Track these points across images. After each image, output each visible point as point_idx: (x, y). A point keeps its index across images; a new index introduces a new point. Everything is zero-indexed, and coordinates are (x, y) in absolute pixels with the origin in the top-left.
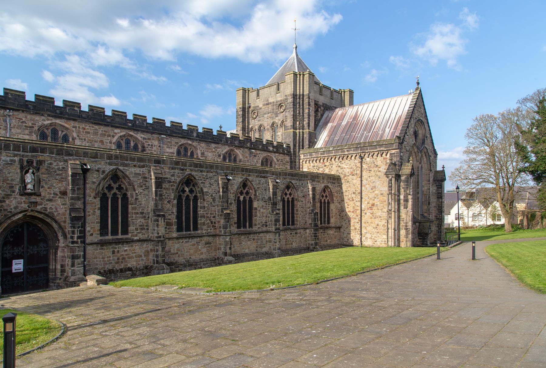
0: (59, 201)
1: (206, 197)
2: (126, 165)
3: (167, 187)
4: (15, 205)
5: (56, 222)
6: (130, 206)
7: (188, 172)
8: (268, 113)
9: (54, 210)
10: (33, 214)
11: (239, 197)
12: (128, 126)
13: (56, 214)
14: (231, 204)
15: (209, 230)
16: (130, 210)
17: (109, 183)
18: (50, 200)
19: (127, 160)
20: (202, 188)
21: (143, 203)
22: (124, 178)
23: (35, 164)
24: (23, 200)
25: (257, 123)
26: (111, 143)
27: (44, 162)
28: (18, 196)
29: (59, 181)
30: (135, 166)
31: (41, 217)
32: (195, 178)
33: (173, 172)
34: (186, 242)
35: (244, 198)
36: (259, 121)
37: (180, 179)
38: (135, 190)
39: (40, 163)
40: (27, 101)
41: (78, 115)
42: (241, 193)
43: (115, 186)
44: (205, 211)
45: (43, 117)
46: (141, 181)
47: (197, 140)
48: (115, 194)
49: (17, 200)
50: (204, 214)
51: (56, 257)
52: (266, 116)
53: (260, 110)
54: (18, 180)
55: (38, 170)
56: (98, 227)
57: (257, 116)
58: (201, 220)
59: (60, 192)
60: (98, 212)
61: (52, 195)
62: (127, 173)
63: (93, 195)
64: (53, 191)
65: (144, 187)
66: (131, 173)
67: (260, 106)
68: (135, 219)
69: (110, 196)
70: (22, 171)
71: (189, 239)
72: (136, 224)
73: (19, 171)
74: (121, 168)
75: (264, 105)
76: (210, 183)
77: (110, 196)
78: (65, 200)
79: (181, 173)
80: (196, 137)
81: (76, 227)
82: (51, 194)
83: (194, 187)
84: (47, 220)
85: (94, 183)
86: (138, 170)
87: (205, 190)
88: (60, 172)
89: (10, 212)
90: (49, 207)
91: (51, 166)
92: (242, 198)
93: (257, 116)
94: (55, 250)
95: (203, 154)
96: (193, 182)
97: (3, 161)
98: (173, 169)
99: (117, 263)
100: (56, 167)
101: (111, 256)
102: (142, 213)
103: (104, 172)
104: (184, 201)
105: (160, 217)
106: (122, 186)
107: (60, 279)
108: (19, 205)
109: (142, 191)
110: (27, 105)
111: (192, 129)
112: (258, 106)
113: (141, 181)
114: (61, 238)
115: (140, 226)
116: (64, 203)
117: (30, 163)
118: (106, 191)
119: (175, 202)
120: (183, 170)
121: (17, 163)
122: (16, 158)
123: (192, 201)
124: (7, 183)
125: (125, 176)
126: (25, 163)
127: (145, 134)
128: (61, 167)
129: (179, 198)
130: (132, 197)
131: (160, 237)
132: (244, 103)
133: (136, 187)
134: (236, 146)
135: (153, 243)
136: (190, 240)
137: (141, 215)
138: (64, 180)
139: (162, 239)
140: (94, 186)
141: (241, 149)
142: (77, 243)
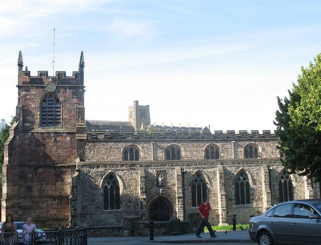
3: (228, 177)
7: (240, 168)
11: (280, 181)
14: (274, 185)
26: (202, 151)
30: (208, 168)
35: (285, 181)
42: (282, 178)
56: (190, 202)
60: (190, 194)
69: (196, 184)
77: (196, 184)
80: (258, 138)
92: (283, 181)
95: (263, 149)
111: (255, 133)
118: (194, 183)
119: (234, 186)
129: (237, 184)
142: (180, 209)
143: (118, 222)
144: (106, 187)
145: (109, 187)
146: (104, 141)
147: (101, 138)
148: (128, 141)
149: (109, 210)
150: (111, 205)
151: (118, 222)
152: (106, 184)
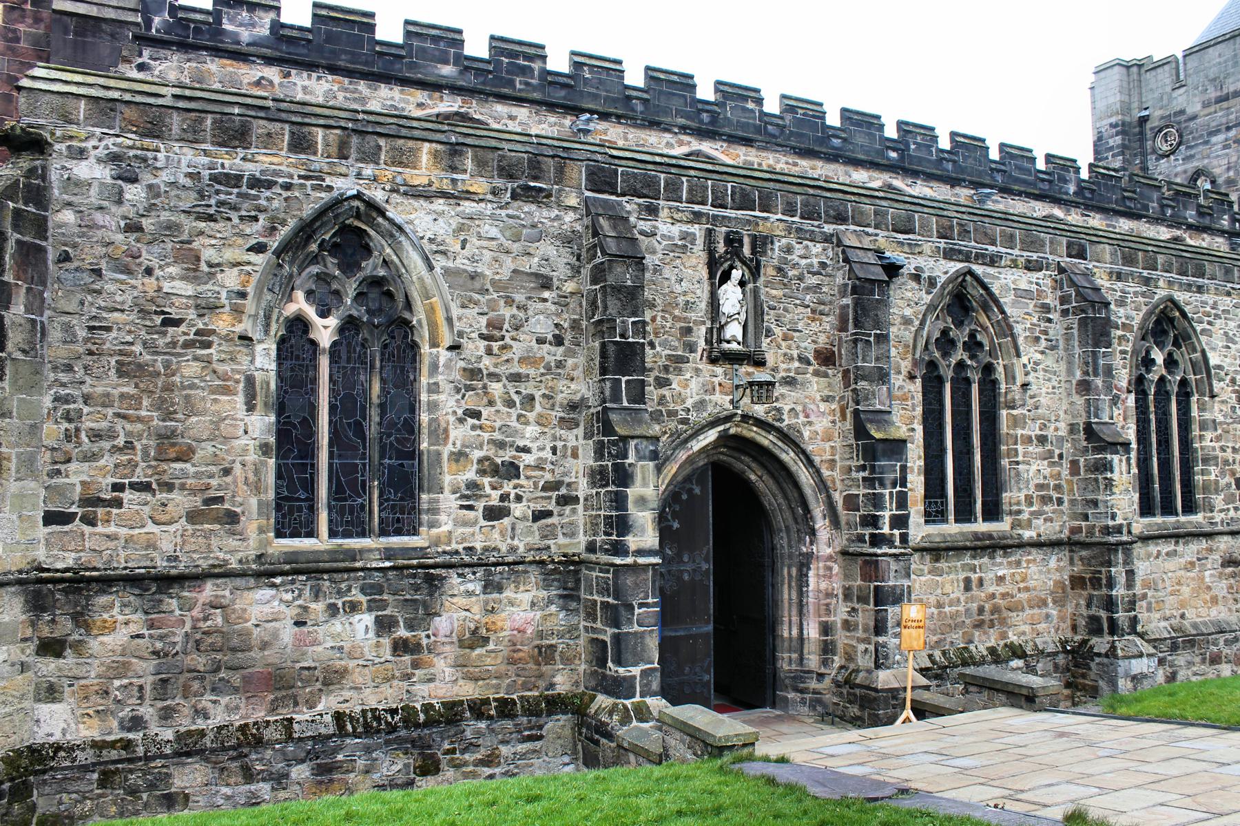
0: (815, 387)
1: (1217, 386)
2: (993, 261)
4: (696, 398)
5: (809, 462)
6: (1004, 413)
7: (1161, 293)
8: (1228, 129)
9: (802, 419)
10: (746, 433)
12: (888, 159)
13: (806, 434)
15: (1232, 513)
16: (1004, 427)
17: (941, 325)
18: (790, 382)
19: (993, 243)
20: (1203, 352)
21: (1044, 401)
22: (986, 308)
23: (746, 250)
24: (716, 380)
25: (1179, 169)
27: (772, 243)
28: (705, 367)
29: (813, 311)
30: (1014, 264)
31: (766, 443)
32: (1184, 314)
33: (1123, 291)
34: (1168, 554)
36: (1187, 159)
37: (1141, 314)
38: (1018, 355)
39: (761, 243)
40: (627, 87)
41: (754, 125)
43: (961, 336)
44: (1218, 439)
45: (668, 136)
46: (1035, 320)
47: (1077, 205)
48: (961, 365)
49: (701, 379)
50: (1214, 449)
51: (801, 594)
52: (1214, 139)
53: (1192, 124)
54: (703, 305)
55: (755, 271)
57: (1179, 144)
58: (1203, 473)
59: (818, 353)
61: (797, 364)
62: (995, 290)
63: (906, 365)
64: (798, 347)
65: (1043, 343)
66: (1005, 288)
67: (1190, 111)
68: (1024, 462)
70: (712, 275)
71: (1177, 543)
72: (1028, 481)
73: (704, 273)
74: (978, 269)
75: (1206, 105)
76: (1226, 334)
78: (830, 385)
79: (1143, 295)
81: (888, 483)
82: (792, 359)
83: (1179, 347)
84: (784, 456)
85: (907, 321)
86: (1025, 280)
87: (1214, 360)
88: (814, 280)
89: (685, 421)
90: (787, 408)
91: (790, 258)
93: (1179, 144)
94: (800, 570)
96: (1174, 327)
97: (663, 236)
98: (1119, 276)
99: (979, 625)
100: (803, 262)
101: (962, 599)
102: (1042, 440)
103: (932, 282)
104: (1151, 397)
105: (1117, 453)
106: (979, 337)
107: (821, 676)
108: (707, 398)
109: (1039, 356)
110: (629, 98)
112: (1182, 112)
113: (1035, 320)
114: (821, 524)
115: (1040, 487)
116: (826, 392)
117: (733, 241)
120: (1147, 281)
121: (700, 241)
122: (697, 230)
123: (1174, 399)
124: (675, 318)
125: (990, 301)
126: (721, 248)
127: (934, 184)
128: (815, 261)
130: (1011, 377)
131: (1118, 529)
132: (1126, 108)
133: (1021, 341)
134: (1190, 227)
135: (1084, 553)
136: (1180, 548)
137: (1040, 449)
138: (827, 309)
139: (1125, 538)
140: (908, 336)
141: (1205, 236)
143: (401, 647)
144: (299, 325)
145: (325, 331)
146: (269, 61)
147: (245, 35)
148: (434, 86)
149: (321, 543)
150: (337, 492)
151: (401, 647)
152: (300, 304)
